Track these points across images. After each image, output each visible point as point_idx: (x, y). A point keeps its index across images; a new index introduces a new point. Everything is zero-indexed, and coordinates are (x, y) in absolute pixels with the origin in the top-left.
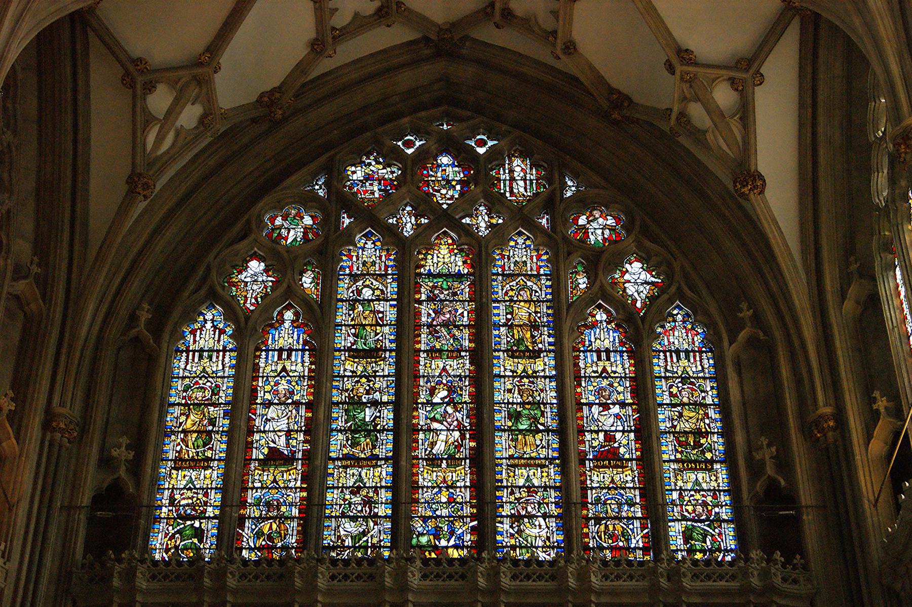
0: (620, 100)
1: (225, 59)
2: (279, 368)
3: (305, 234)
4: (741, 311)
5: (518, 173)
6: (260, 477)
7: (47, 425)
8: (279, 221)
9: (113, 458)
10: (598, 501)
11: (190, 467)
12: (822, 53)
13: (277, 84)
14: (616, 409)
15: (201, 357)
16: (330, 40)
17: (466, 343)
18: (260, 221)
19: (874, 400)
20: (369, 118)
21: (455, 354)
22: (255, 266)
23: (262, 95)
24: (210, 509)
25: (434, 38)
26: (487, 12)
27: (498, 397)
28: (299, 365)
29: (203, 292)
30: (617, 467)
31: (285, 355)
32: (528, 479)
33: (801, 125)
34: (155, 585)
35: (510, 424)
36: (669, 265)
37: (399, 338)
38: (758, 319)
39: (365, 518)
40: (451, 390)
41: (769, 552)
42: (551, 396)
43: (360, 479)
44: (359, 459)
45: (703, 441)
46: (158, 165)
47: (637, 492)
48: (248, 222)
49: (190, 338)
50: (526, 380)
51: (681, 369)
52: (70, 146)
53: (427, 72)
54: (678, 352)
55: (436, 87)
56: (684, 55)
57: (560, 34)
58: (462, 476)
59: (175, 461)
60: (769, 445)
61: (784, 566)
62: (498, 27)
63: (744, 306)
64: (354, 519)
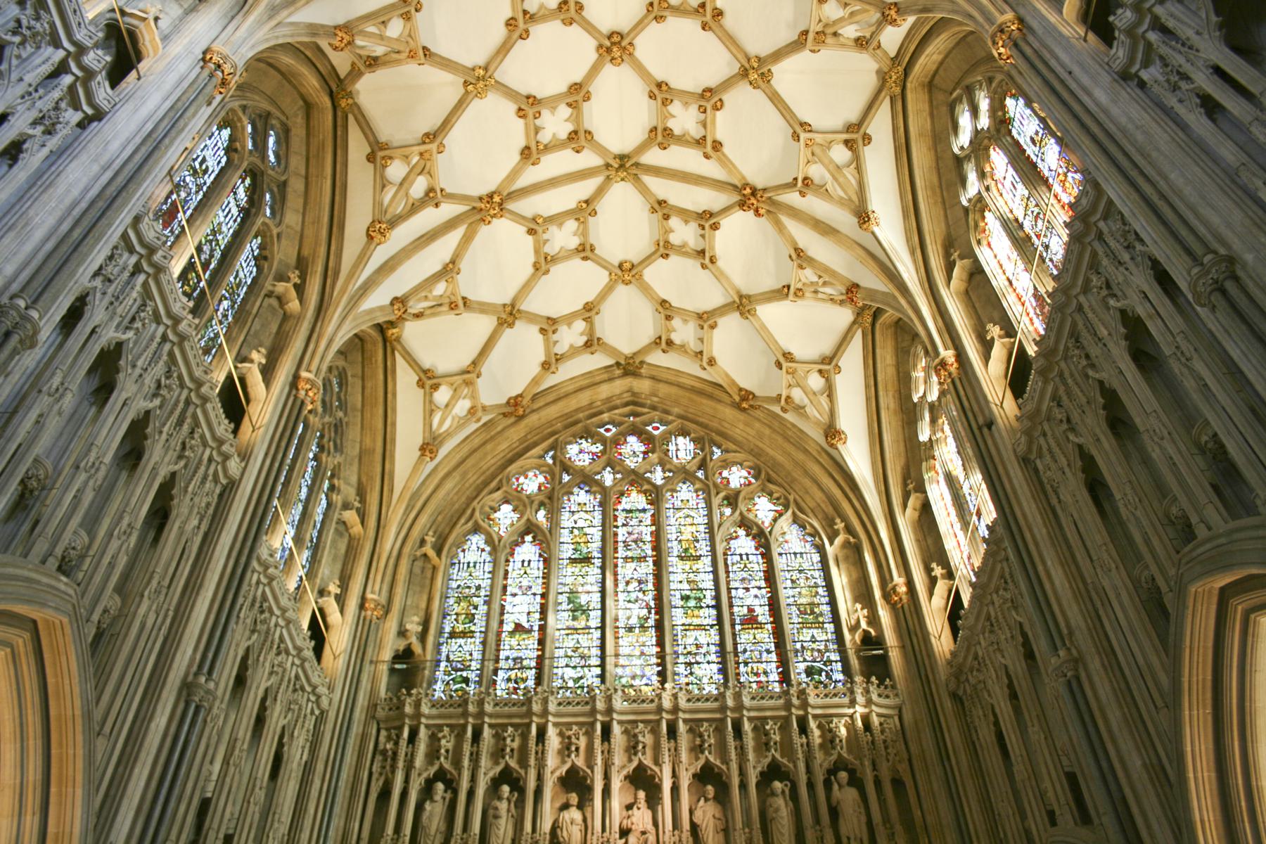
0: (747, 395)
1: (484, 369)
2: (522, 572)
3: (540, 487)
4: (836, 524)
5: (681, 447)
6: (507, 642)
7: (362, 606)
8: (522, 479)
9: (407, 631)
10: (745, 651)
11: (460, 637)
12: (878, 351)
13: (520, 392)
14: (754, 591)
15: (468, 567)
16: (554, 361)
17: (650, 552)
18: (509, 480)
19: (932, 570)
20: (581, 415)
21: (642, 559)
22: (506, 508)
23: (510, 399)
24: (473, 664)
25: (623, 362)
26: (657, 342)
27: (673, 586)
28: (537, 569)
29: (470, 524)
30: (757, 628)
31: (526, 564)
32: (696, 639)
33: (868, 399)
34: (434, 711)
35: (682, 603)
36: (786, 499)
37: (603, 550)
38: (849, 529)
39: (582, 667)
40: (640, 582)
41: (867, 676)
42: (710, 585)
43: (578, 642)
44: (576, 629)
45: (816, 610)
46: (440, 439)
47: (773, 645)
48: (501, 481)
49: (461, 555)
50: (691, 575)
51: (797, 566)
52: (380, 425)
53: (620, 386)
54: (795, 554)
55: (625, 395)
56: (788, 356)
57: (705, 353)
58: (650, 637)
59: (450, 633)
60: (862, 609)
61: (878, 686)
62: (664, 352)
63: (838, 520)
64: (575, 667)
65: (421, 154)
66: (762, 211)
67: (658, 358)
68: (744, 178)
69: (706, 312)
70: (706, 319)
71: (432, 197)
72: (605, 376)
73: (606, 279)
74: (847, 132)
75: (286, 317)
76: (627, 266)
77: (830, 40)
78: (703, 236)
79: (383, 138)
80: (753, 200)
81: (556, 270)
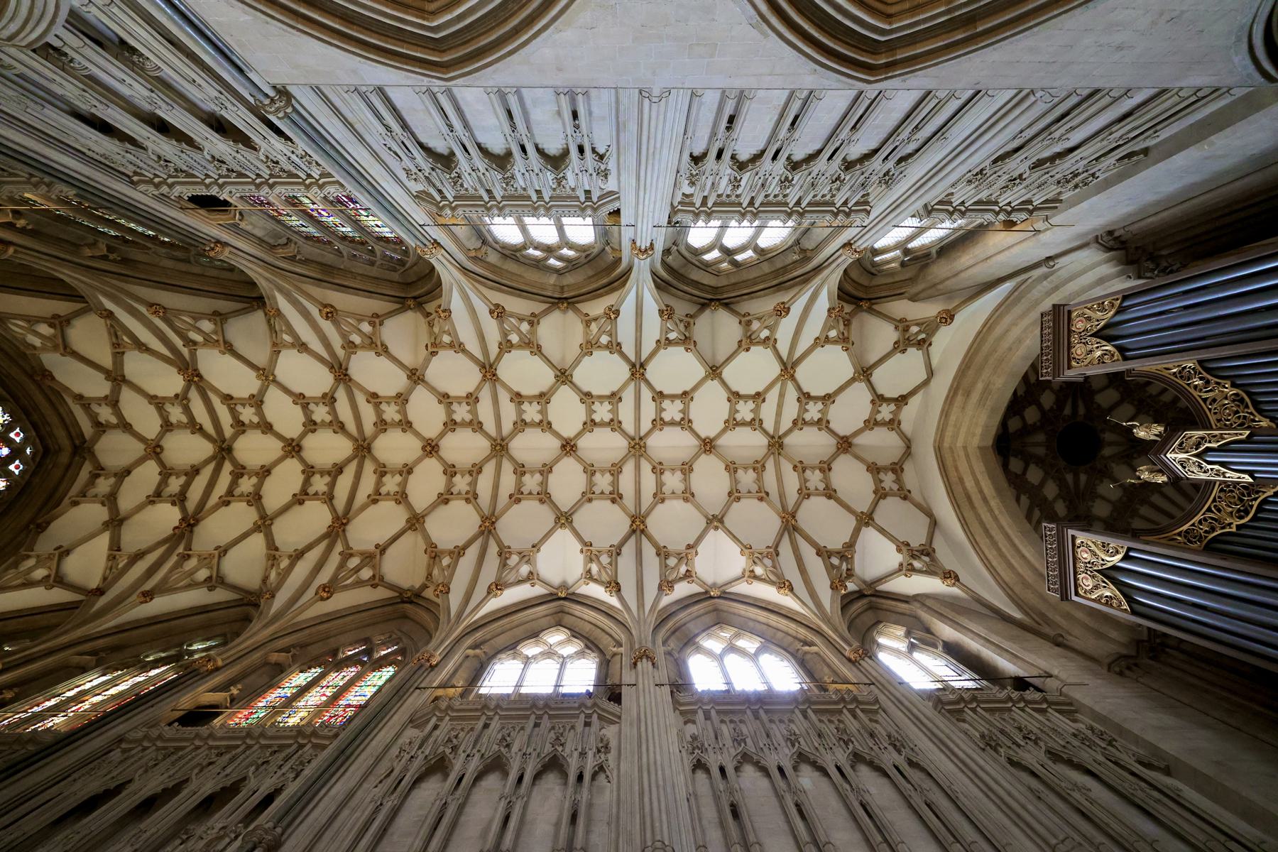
0: (42, 528)
1: (68, 359)
53: (64, 442)
65: (217, 341)
66: (176, 531)
67: (86, 470)
68: (203, 519)
69: (115, 499)
70: (111, 499)
71: (189, 343)
72: (74, 434)
73: (149, 438)
74: (217, 576)
75: (77, 246)
76: (158, 450)
77: (270, 562)
78: (170, 496)
79: (230, 321)
80: (184, 525)
81: (152, 410)
